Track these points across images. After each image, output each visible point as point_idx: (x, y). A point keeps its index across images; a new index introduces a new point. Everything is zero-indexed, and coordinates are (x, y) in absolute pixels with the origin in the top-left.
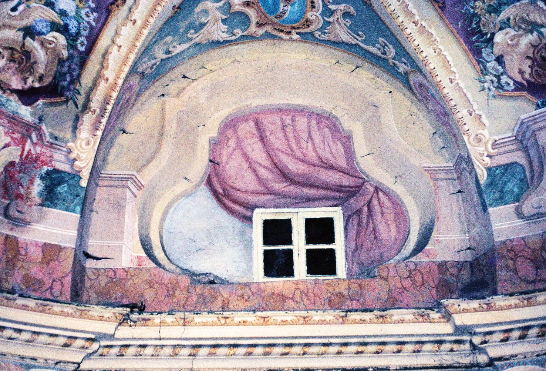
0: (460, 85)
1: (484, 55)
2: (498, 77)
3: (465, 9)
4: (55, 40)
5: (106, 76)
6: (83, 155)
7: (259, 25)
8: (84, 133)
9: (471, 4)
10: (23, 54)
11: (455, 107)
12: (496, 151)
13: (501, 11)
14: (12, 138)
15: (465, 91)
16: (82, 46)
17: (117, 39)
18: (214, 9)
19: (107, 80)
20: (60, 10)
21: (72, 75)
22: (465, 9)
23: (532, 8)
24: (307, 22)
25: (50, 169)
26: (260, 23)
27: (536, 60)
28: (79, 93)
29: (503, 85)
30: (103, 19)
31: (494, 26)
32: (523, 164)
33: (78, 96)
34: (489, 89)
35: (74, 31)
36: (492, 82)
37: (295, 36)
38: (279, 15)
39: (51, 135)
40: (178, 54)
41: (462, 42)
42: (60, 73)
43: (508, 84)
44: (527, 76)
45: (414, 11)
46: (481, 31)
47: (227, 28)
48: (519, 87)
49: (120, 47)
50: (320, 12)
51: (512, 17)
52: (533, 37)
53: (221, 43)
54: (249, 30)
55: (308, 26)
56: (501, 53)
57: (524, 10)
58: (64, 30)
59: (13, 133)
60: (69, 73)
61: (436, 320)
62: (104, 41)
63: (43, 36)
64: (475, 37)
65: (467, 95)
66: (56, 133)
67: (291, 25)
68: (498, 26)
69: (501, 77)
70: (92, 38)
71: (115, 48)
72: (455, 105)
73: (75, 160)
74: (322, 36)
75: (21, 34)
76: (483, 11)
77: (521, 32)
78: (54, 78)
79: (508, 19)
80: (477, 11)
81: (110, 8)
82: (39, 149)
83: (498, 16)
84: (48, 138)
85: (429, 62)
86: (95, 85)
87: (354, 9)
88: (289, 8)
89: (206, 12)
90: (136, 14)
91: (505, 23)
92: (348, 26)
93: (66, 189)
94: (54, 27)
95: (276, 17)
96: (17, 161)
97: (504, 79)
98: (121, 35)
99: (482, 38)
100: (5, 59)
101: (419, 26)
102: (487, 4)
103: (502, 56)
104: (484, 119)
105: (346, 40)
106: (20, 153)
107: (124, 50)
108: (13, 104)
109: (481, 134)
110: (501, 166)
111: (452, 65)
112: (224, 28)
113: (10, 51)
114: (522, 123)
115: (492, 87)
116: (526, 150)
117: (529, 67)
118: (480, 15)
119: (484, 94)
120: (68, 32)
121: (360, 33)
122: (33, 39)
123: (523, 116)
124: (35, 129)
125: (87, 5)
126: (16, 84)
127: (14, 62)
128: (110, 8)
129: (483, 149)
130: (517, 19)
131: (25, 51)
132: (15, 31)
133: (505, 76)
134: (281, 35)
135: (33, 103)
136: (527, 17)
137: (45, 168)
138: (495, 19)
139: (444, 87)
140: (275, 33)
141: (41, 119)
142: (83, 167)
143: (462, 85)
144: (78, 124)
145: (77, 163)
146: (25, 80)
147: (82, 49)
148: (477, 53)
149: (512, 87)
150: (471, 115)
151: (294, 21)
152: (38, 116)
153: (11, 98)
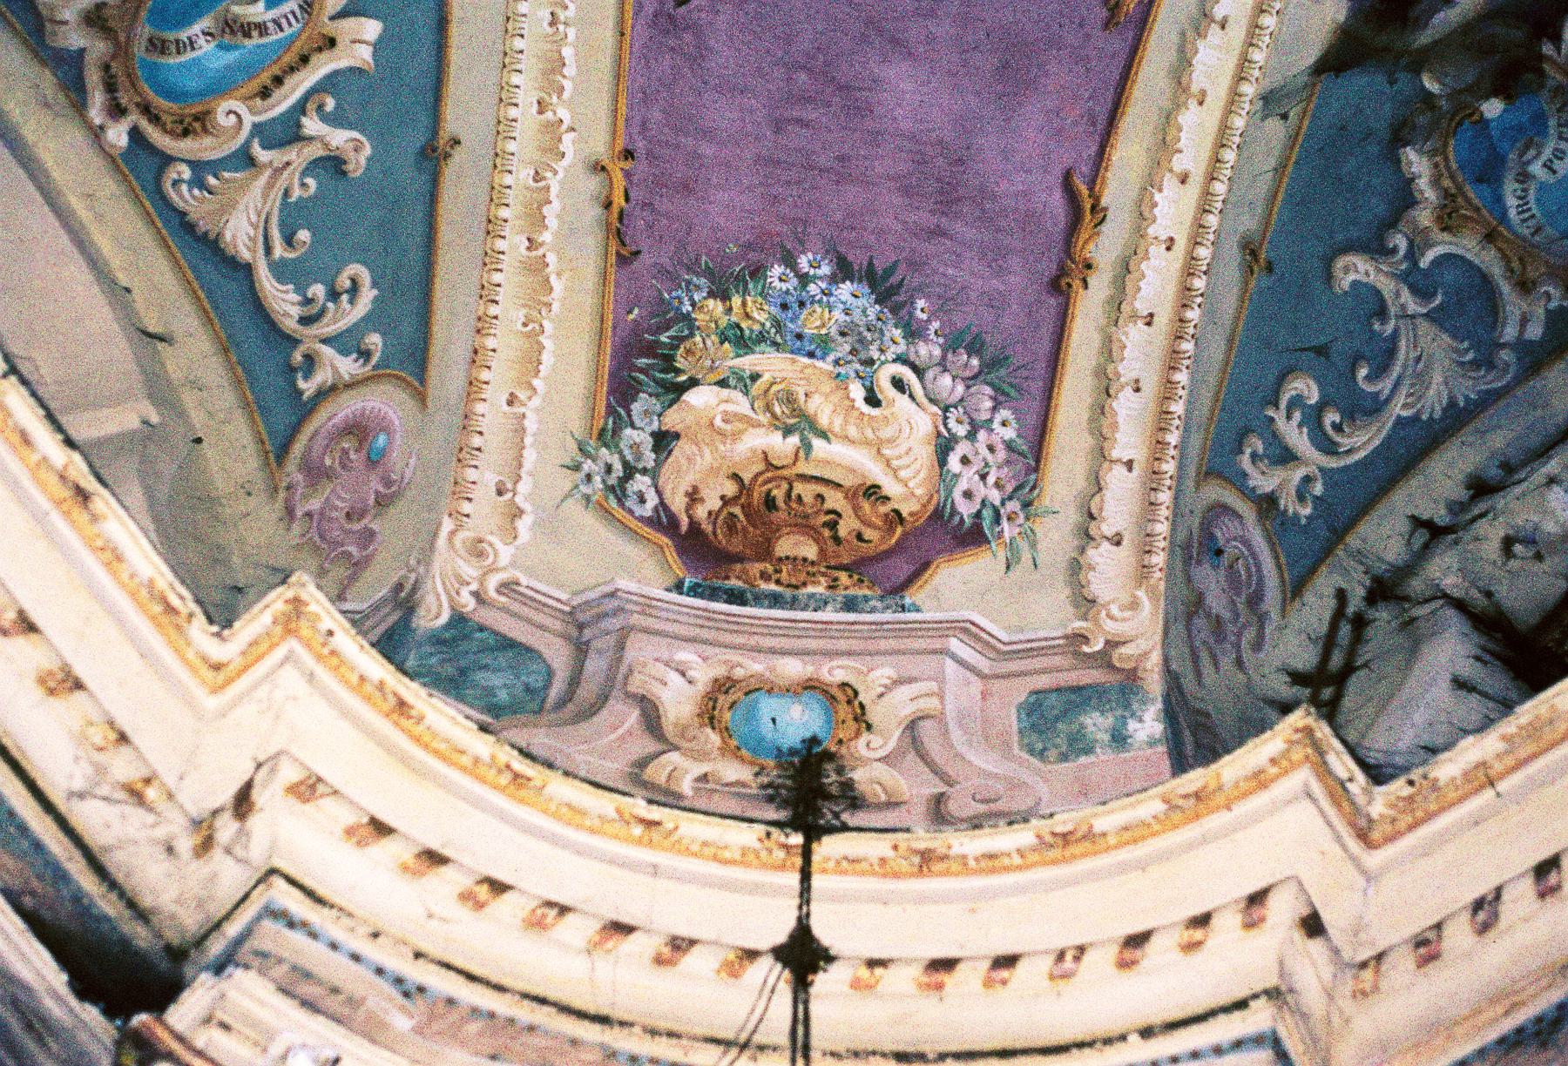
0: (527, 423)
1: (636, 407)
2: (630, 471)
3: (674, 294)
9: (696, 298)
11: (477, 453)
12: (503, 599)
13: (753, 352)
15: (528, 440)
22: (674, 294)
23: (827, 386)
26: (107, 12)
27: (750, 491)
29: (629, 492)
31: (712, 369)
32: (555, 666)
34: (589, 477)
36: (609, 469)
37: (118, 135)
38: (164, 42)
41: (609, 351)
43: (642, 500)
44: (701, 512)
45: (552, 222)
46: (669, 359)
48: (664, 521)
50: (257, 119)
51: (766, 377)
52: (782, 446)
55: (186, 133)
56: (678, 428)
57: (808, 380)
61: (190, 655)
64: (644, 361)
65: (525, 453)
67: (151, 95)
68: (713, 377)
69: (638, 476)
72: (479, 449)
74: (184, 188)
76: (713, 325)
77: (764, 418)
79: (755, 377)
80: (700, 318)
83: (738, 356)
85: (492, 331)
87: (369, 159)
88: (206, 47)
91: (740, 379)
92: (293, 199)
95: (150, 40)
97: (641, 483)
99: (662, 371)
101: (534, 253)
102: (734, 319)
103: (677, 436)
104: (524, 525)
105: (234, 236)
109: (491, 545)
110: (496, 633)
111: (541, 374)
114: (613, 595)
115: (597, 479)
116: (581, 650)
117: (722, 497)
118: (698, 328)
119: (566, 481)
121: (304, 235)
123: (624, 583)
129: (475, 573)
130: (775, 388)
133: (647, 480)
134: (97, 99)
136: (802, 398)
138: (724, 358)
139: (484, 400)
140: (93, 77)
143: (531, 424)
148: (622, 391)
149: (647, 510)
150: (500, 493)
151: (170, 94)
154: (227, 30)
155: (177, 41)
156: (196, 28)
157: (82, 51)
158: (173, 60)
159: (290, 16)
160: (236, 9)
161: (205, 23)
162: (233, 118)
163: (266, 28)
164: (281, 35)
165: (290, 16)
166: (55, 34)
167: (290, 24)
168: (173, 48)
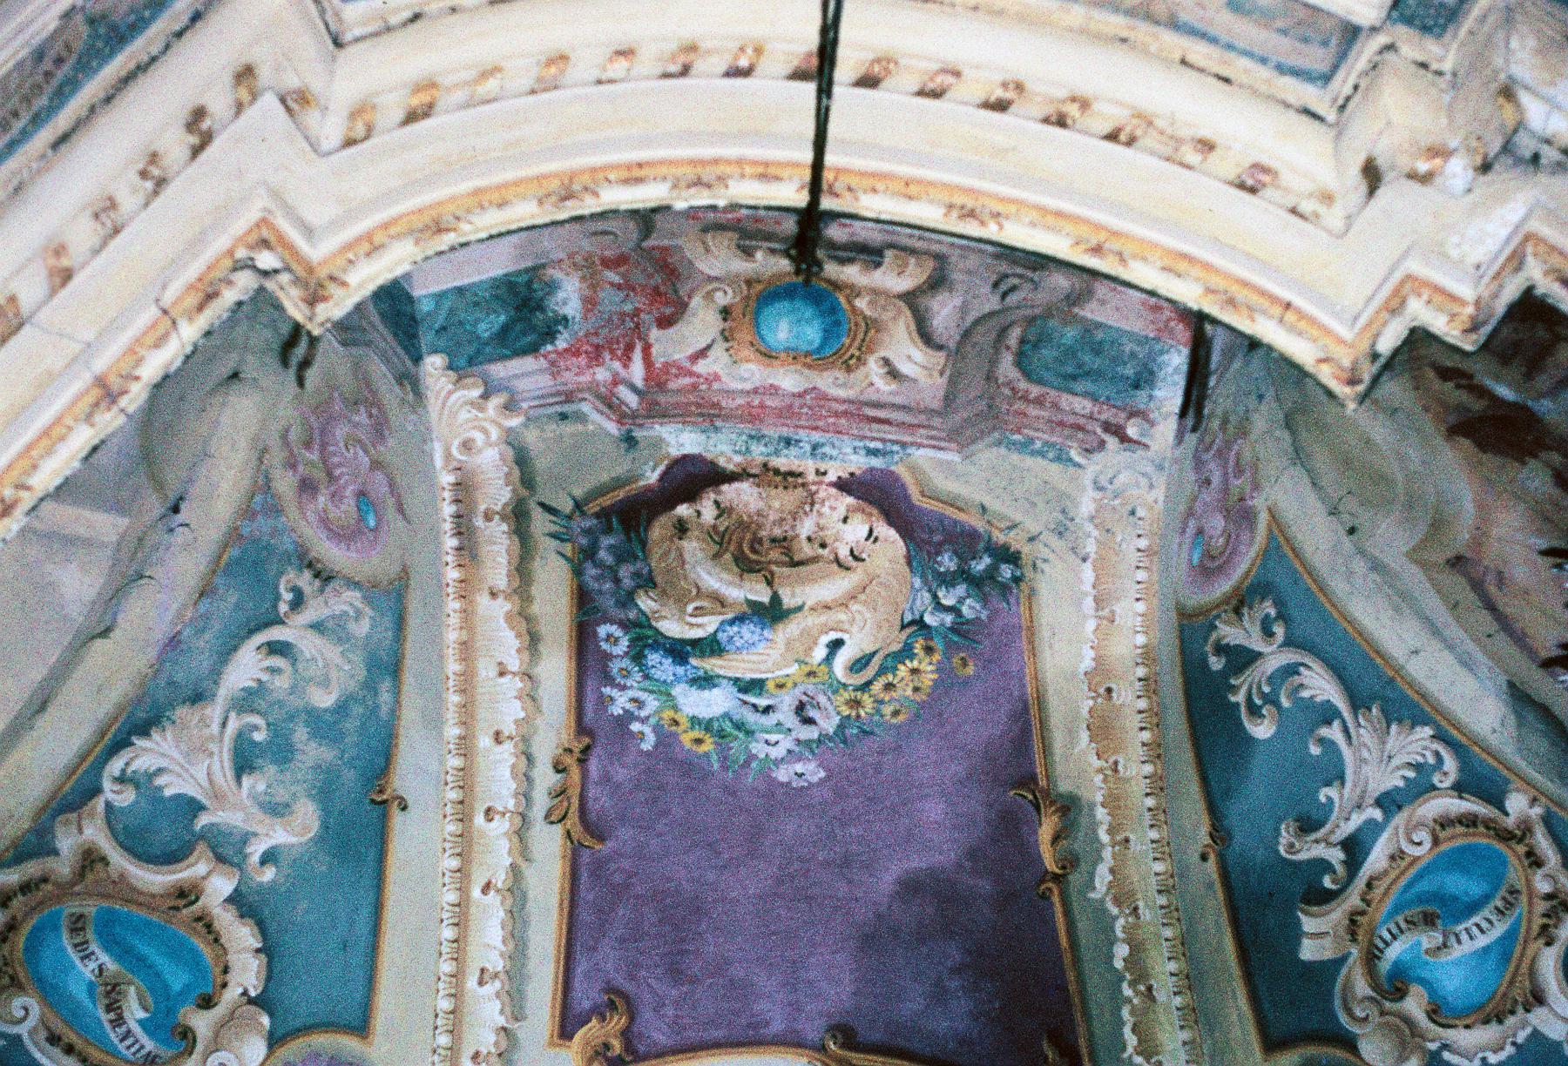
4: (693, 620)
5: (500, 600)
6: (468, 416)
7: (91, 859)
8: (491, 462)
10: (758, 562)
14: (691, 374)
16: (609, 636)
17: (520, 685)
18: (260, 829)
19: (493, 595)
20: (715, 686)
21: (599, 565)
24: (12, 978)
25: (549, 347)
26: (99, 866)
28: (554, 536)
30: (589, 707)
33: (554, 528)
35: (649, 657)
38: (83, 929)
39: (581, 418)
40: (235, 649)
42: (636, 558)
47: (160, 789)
49: (502, 674)
53: (130, 734)
54: (100, 821)
58: (679, 651)
59: (695, 387)
60: (610, 567)
62: (556, 668)
63: (730, 616)
66: (568, 428)
67: (25, 930)
70: (591, 661)
71: (514, 664)
73: (485, 396)
75: (788, 601)
78: (644, 544)
81: (587, 740)
82: (602, 375)
84: (586, 408)
86: (522, 570)
88: (88, 970)
89: (276, 810)
90: (506, 755)
93: (482, 326)
94: (711, 646)
95: (82, 916)
96: (654, 333)
98: (519, 698)
100: (803, 536)
106: (654, 351)
107: (485, 670)
108: (726, 448)
112: (172, 786)
113: (796, 558)
120: (666, 650)
122: (751, 604)
124: (634, 415)
125: (653, 721)
126: (743, 495)
127: (774, 540)
128: (587, 740)
131: (759, 571)
132: (809, 603)
135: (669, 468)
137: (561, 344)
140: (32, 869)
141: (630, 441)
142: (450, 393)
144: (517, 472)
145: (476, 393)
146: (722, 510)
147: (602, 631)
151: (32, 948)
152: (641, 445)
153: (738, 459)
154: (109, 988)
155: (86, 942)
156: (104, 958)
157: (55, 852)
158: (66, 940)
159: (137, 1046)
160: (132, 989)
161: (112, 966)
162: (22, 1013)
163: (119, 1026)
164: (116, 1041)
165: (137, 1046)
166: (67, 823)
167: (128, 1048)
168: (77, 941)
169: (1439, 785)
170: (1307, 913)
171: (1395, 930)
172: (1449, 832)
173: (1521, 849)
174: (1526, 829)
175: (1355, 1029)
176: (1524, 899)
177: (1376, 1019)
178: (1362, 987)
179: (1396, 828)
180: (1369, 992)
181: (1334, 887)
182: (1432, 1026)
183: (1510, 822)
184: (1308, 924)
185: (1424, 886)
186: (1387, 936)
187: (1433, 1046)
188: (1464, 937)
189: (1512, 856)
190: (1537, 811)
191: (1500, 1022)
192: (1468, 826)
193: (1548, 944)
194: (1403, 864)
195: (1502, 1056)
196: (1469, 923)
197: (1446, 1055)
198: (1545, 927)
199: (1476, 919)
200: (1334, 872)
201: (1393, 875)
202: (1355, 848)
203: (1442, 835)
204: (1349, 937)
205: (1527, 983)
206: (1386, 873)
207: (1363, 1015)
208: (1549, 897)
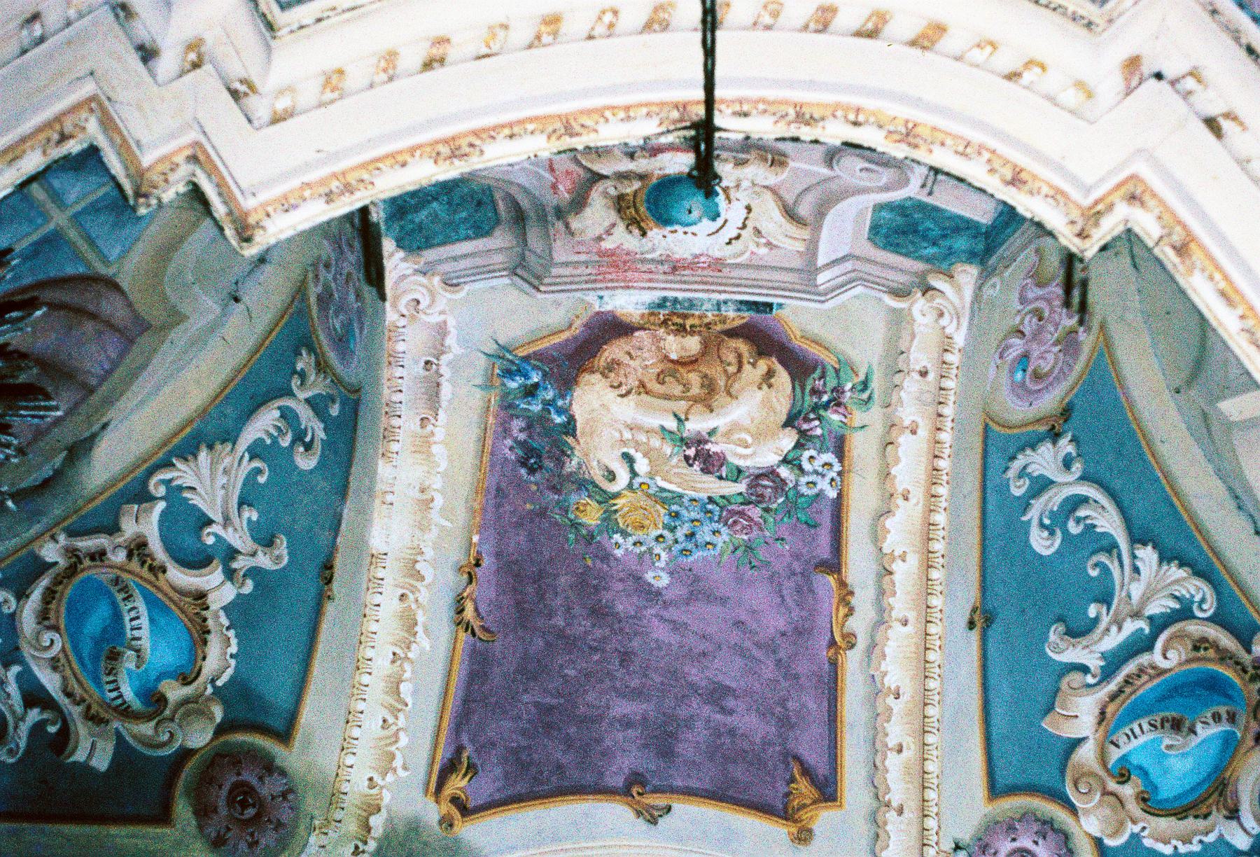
169: (11, 610)
170: (72, 753)
171: (112, 686)
172: (52, 615)
173: (87, 562)
174: (71, 552)
175: (176, 745)
176: (125, 576)
177: (173, 726)
178: (147, 729)
179: (33, 657)
180: (153, 723)
181: (58, 726)
182: (195, 685)
183: (63, 563)
184: (80, 756)
185: (87, 648)
186: (115, 694)
187: (210, 690)
188: (136, 633)
189: (91, 572)
190: (62, 538)
191: (208, 632)
192: (53, 598)
193: (164, 571)
194: (63, 661)
195: (234, 642)
196: (128, 626)
197: (219, 683)
198: (151, 568)
199: (127, 619)
200: (48, 720)
201: (68, 672)
202: (35, 696)
203: (52, 622)
204: (103, 725)
205: (188, 600)
206: (64, 678)
207: (168, 735)
208: (130, 555)
